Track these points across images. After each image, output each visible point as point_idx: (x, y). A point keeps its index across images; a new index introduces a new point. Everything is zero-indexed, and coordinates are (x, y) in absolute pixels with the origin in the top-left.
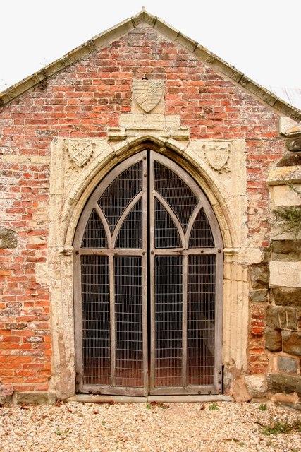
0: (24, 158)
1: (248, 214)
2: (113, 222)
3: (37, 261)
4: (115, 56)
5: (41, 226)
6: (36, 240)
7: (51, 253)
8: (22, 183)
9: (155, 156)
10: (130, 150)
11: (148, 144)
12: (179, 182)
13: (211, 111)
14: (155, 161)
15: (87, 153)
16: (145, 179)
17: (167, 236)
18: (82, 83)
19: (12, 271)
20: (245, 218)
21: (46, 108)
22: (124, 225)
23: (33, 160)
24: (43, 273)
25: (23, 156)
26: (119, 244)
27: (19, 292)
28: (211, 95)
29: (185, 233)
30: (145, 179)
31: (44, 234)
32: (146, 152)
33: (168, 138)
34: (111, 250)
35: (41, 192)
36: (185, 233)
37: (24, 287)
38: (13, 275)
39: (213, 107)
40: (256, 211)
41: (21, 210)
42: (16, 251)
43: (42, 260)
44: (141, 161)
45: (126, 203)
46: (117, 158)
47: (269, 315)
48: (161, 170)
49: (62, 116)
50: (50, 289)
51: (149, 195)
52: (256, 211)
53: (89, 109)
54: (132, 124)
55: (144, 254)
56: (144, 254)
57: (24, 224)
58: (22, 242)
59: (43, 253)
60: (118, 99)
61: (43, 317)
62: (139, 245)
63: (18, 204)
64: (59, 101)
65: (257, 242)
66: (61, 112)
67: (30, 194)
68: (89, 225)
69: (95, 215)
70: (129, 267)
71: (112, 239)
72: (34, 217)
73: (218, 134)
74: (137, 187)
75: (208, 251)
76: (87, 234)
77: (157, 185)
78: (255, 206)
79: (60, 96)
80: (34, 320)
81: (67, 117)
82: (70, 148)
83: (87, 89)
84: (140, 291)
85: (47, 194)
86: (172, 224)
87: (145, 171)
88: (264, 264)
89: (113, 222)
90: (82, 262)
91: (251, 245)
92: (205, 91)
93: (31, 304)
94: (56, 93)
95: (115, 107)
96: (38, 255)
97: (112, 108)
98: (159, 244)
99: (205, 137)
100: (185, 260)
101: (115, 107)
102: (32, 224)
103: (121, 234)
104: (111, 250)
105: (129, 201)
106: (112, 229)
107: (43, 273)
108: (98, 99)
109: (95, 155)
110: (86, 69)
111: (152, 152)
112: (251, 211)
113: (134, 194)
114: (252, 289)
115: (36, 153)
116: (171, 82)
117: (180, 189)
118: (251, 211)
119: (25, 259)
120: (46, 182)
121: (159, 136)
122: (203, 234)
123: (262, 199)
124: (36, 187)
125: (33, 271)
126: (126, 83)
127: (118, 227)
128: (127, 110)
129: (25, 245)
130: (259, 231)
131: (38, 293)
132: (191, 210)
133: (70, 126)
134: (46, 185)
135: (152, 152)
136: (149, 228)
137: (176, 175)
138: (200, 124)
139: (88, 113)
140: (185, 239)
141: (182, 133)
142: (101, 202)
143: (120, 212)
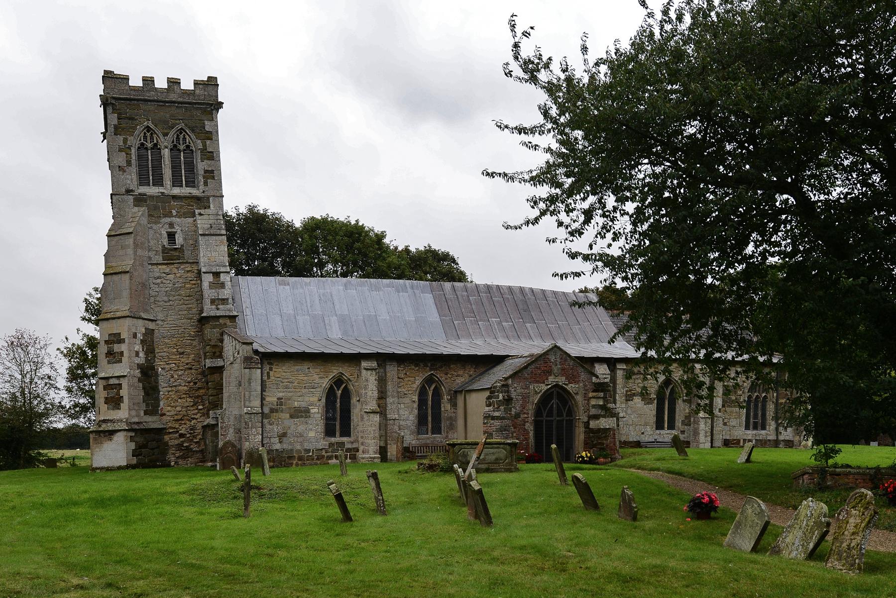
11: (557, 386)
17: (560, 414)
24: (527, 425)
46: (548, 390)
58: (522, 416)
61: (527, 439)
64: (532, 372)
71: (545, 415)
74: (552, 399)
88: (588, 422)
98: (558, 416)
104: (544, 418)
122: (570, 413)
131: (526, 432)
136: (555, 412)
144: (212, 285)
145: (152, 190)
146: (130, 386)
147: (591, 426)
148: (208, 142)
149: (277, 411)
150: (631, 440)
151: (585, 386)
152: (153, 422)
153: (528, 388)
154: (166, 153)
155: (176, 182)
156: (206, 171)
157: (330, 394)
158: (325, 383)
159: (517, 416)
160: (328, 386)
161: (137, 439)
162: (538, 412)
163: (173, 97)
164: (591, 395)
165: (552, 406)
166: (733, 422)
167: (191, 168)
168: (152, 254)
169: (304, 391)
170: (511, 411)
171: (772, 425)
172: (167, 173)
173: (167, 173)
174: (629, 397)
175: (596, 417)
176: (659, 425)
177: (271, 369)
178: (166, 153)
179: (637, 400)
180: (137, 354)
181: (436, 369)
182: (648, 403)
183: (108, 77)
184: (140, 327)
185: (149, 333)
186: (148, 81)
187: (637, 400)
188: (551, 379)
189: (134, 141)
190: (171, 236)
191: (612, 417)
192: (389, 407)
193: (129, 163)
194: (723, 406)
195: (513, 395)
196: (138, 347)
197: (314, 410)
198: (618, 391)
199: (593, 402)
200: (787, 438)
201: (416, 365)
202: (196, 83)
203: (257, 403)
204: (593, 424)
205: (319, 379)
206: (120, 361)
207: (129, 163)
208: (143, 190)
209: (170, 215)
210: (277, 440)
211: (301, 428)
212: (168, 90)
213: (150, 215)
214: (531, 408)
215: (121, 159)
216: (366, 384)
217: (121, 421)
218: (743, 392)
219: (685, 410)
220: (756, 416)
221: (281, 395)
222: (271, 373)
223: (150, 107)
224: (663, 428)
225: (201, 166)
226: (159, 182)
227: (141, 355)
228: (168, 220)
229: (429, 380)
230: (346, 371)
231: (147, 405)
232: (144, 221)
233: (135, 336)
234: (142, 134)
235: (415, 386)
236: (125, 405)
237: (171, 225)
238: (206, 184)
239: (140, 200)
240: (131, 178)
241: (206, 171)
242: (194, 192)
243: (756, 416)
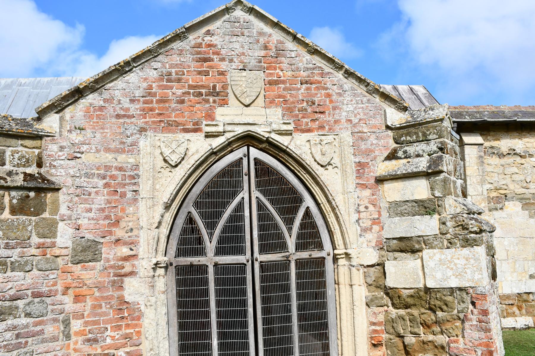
0: (110, 156)
1: (359, 212)
2: (211, 227)
3: (125, 275)
4: (210, 46)
5: (130, 234)
6: (125, 251)
7: (144, 265)
8: (106, 185)
9: (255, 153)
10: (228, 147)
11: (249, 139)
12: (282, 180)
13: (314, 104)
14: (255, 159)
15: (182, 150)
16: (246, 178)
17: (271, 240)
18: (174, 74)
19: (96, 289)
20: (356, 216)
21: (132, 101)
22: (224, 231)
23: (119, 160)
25: (107, 155)
26: (219, 252)
27: (105, 314)
28: (314, 86)
29: (290, 236)
30: (246, 178)
31: (132, 244)
32: (246, 148)
33: (270, 132)
34: (210, 258)
35: (129, 195)
36: (290, 236)
37: (111, 307)
38: (97, 294)
39: (316, 99)
40: (366, 207)
41: (107, 217)
42: (98, 265)
43: (132, 274)
44: (242, 158)
45: (225, 205)
47: (391, 322)
48: (262, 169)
49: (152, 110)
50: (143, 308)
51: (249, 195)
52: (366, 207)
53: (182, 102)
54: (231, 118)
55: (248, 261)
56: (248, 261)
57: (110, 233)
58: (110, 253)
59: (133, 266)
60: (214, 92)
62: (240, 251)
63: (103, 210)
65: (370, 241)
66: (150, 106)
67: (117, 197)
68: (184, 231)
69: (190, 220)
70: (231, 280)
71: (210, 246)
72: (122, 224)
73: (322, 127)
74: (236, 188)
75: (316, 254)
76: (182, 242)
77: (258, 185)
78: (366, 202)
79: (150, 87)
80: (124, 346)
81: (157, 111)
82: (162, 145)
83: (179, 80)
84: (244, 303)
85: (137, 197)
86: (276, 226)
87: (245, 170)
89: (211, 227)
90: (177, 274)
91: (365, 245)
92: (306, 83)
93: (119, 327)
94: (145, 85)
95: (211, 100)
96: (128, 268)
97: (207, 101)
98: (263, 250)
99: (309, 131)
100: (293, 266)
101: (211, 100)
102: (119, 233)
103: (221, 241)
104: (210, 258)
105: (229, 203)
106: (211, 235)
107: (134, 290)
108: (192, 91)
109: (189, 153)
110: (178, 59)
111: (251, 148)
112: (362, 208)
113: (234, 195)
114: (368, 294)
115: (123, 151)
116: (271, 74)
117: (285, 188)
118: (362, 208)
119: (112, 275)
120: (135, 184)
121: (261, 131)
123: (373, 195)
124: (123, 190)
125: (121, 288)
126: (222, 73)
127: (218, 231)
128: (224, 103)
129: (111, 257)
130: (371, 229)
131: (127, 314)
132: (296, 210)
133: (160, 121)
134: (135, 188)
135: (251, 148)
137: (278, 173)
138: (303, 117)
139: (182, 106)
140: (291, 242)
141: (285, 127)
142: (197, 205)
143: (219, 215)
147: (390, 282)
151: (359, 137)
159: (86, 252)
164: (384, 168)
165: (237, 216)
170: (49, 230)
175: (408, 246)
179: (513, 207)
187: (513, 207)
191: (468, 243)
195: (59, 173)
204: (403, 273)
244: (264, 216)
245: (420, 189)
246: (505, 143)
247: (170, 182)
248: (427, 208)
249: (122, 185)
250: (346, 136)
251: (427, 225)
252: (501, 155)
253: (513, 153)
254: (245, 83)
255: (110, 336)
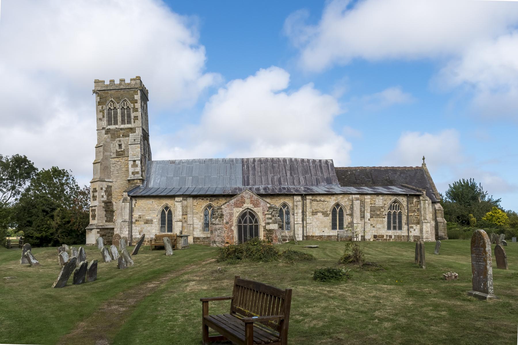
7: (234, 225)
10: (245, 210)
11: (248, 209)
24: (233, 228)
34: (242, 224)
48: (250, 212)
51: (248, 216)
54: (246, 206)
58: (230, 223)
70: (245, 227)
71: (243, 222)
104: (242, 224)
107: (233, 228)
117: (253, 215)
122: (256, 222)
131: (232, 231)
136: (248, 221)
144: (132, 166)
145: (112, 127)
146: (98, 210)
148: (136, 104)
149: (138, 221)
150: (317, 235)
152: (110, 225)
153: (233, 210)
154: (119, 111)
155: (123, 122)
156: (135, 117)
157: (163, 213)
158: (160, 208)
159: (227, 223)
160: (161, 210)
161: (101, 233)
162: (240, 222)
163: (122, 87)
164: (266, 213)
166: (379, 226)
167: (129, 116)
168: (112, 154)
169: (150, 212)
170: (223, 220)
171: (405, 227)
172: (119, 119)
173: (119, 119)
174: (314, 213)
175: (269, 224)
176: (334, 227)
177: (136, 203)
178: (119, 111)
179: (320, 214)
180: (103, 196)
181: (212, 201)
182: (326, 216)
183: (97, 82)
184: (105, 185)
185: (109, 187)
186: (112, 81)
187: (320, 214)
188: (245, 205)
189: (106, 108)
190: (120, 145)
192: (189, 219)
193: (104, 117)
194: (371, 217)
195: (224, 214)
196: (103, 193)
197: (155, 220)
198: (307, 210)
199: (267, 216)
200: (416, 235)
201: (203, 199)
202: (131, 80)
203: (127, 217)
204: (268, 227)
205: (157, 205)
206: (96, 200)
207: (104, 117)
208: (109, 127)
209: (119, 137)
210: (138, 234)
211: (149, 228)
212: (120, 84)
213: (112, 138)
214: (235, 220)
215: (101, 116)
216: (177, 207)
217: (94, 225)
218: (385, 210)
219: (348, 219)
220: (395, 222)
221: (140, 214)
222: (136, 204)
223: (113, 92)
224: (336, 229)
225: (133, 115)
226: (116, 123)
227: (105, 197)
228: (119, 139)
229: (210, 206)
230: (169, 202)
231: (107, 218)
232: (108, 140)
233: (102, 189)
234: (110, 104)
235: (202, 209)
236: (96, 218)
237: (120, 141)
238: (134, 122)
239: (108, 131)
240: (104, 123)
241: (135, 117)
242: (129, 126)
243: (395, 222)
244: (250, 219)
245: (270, 216)
246: (318, 198)
247: (237, 214)
248: (271, 219)
249: (231, 215)
250: (261, 208)
251: (270, 221)
252: (317, 201)
253: (320, 201)
254: (247, 201)
255: (230, 233)
